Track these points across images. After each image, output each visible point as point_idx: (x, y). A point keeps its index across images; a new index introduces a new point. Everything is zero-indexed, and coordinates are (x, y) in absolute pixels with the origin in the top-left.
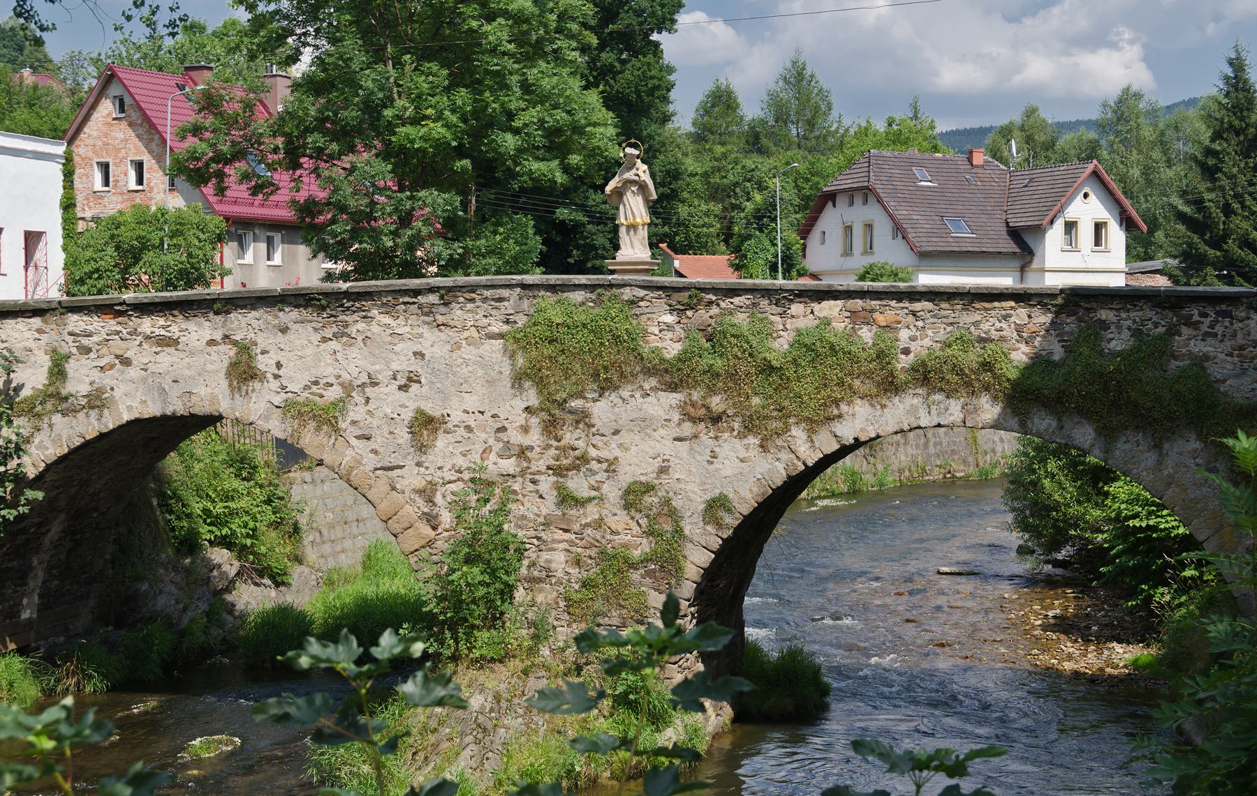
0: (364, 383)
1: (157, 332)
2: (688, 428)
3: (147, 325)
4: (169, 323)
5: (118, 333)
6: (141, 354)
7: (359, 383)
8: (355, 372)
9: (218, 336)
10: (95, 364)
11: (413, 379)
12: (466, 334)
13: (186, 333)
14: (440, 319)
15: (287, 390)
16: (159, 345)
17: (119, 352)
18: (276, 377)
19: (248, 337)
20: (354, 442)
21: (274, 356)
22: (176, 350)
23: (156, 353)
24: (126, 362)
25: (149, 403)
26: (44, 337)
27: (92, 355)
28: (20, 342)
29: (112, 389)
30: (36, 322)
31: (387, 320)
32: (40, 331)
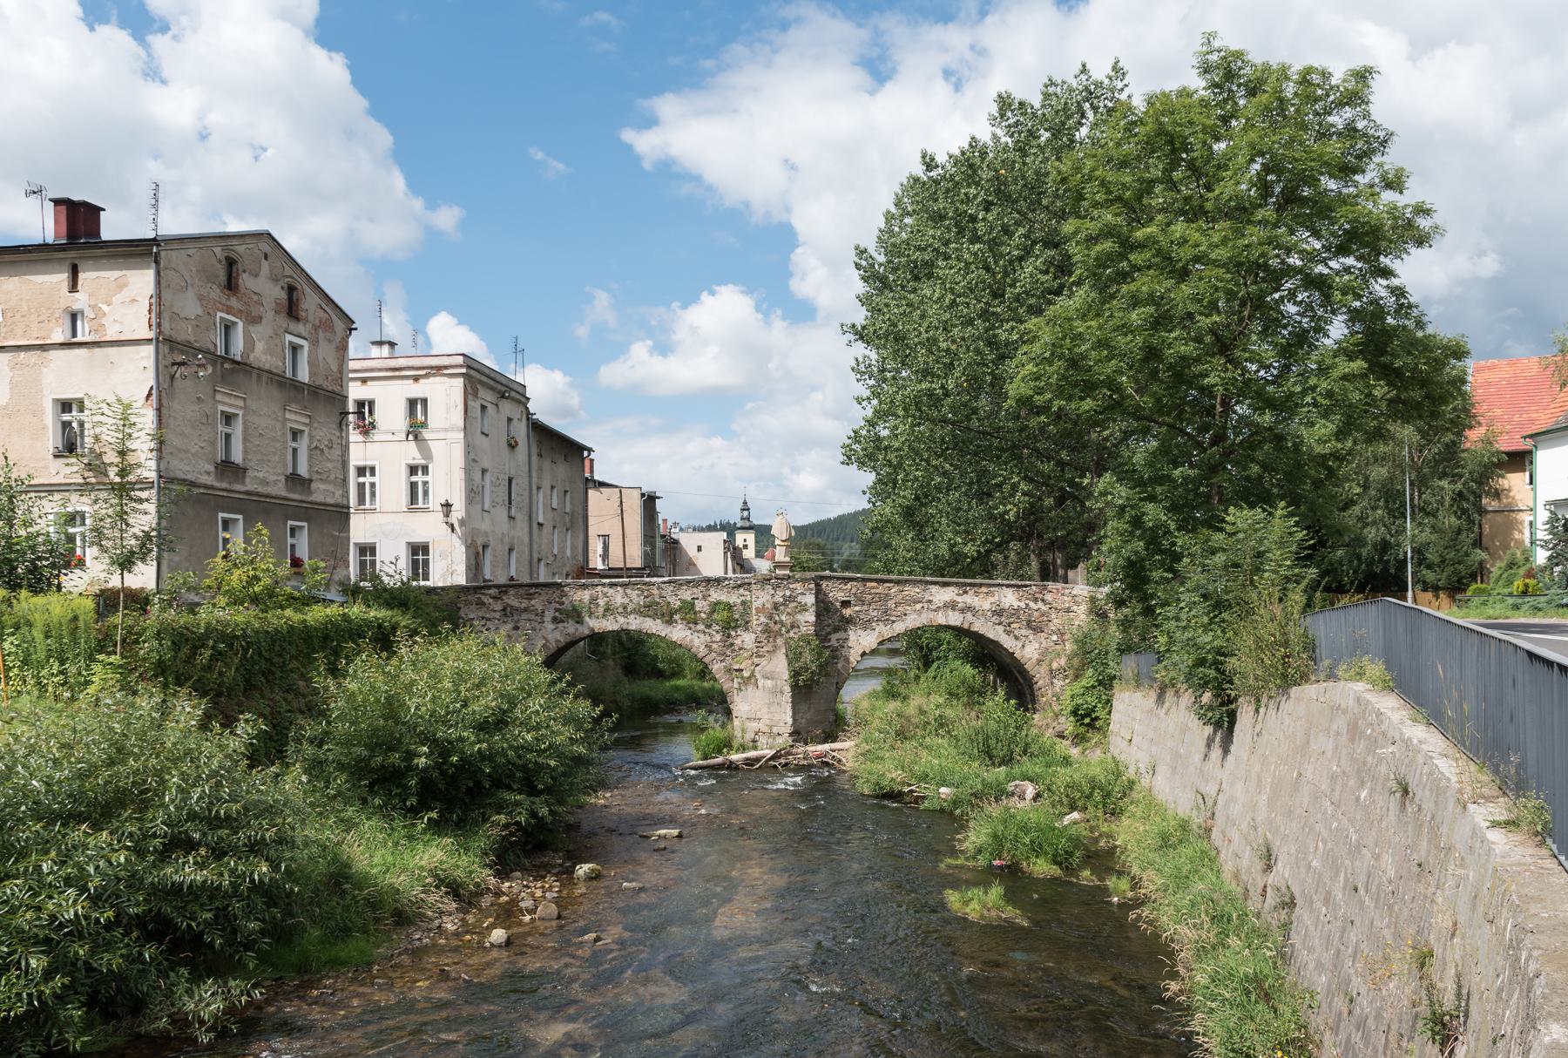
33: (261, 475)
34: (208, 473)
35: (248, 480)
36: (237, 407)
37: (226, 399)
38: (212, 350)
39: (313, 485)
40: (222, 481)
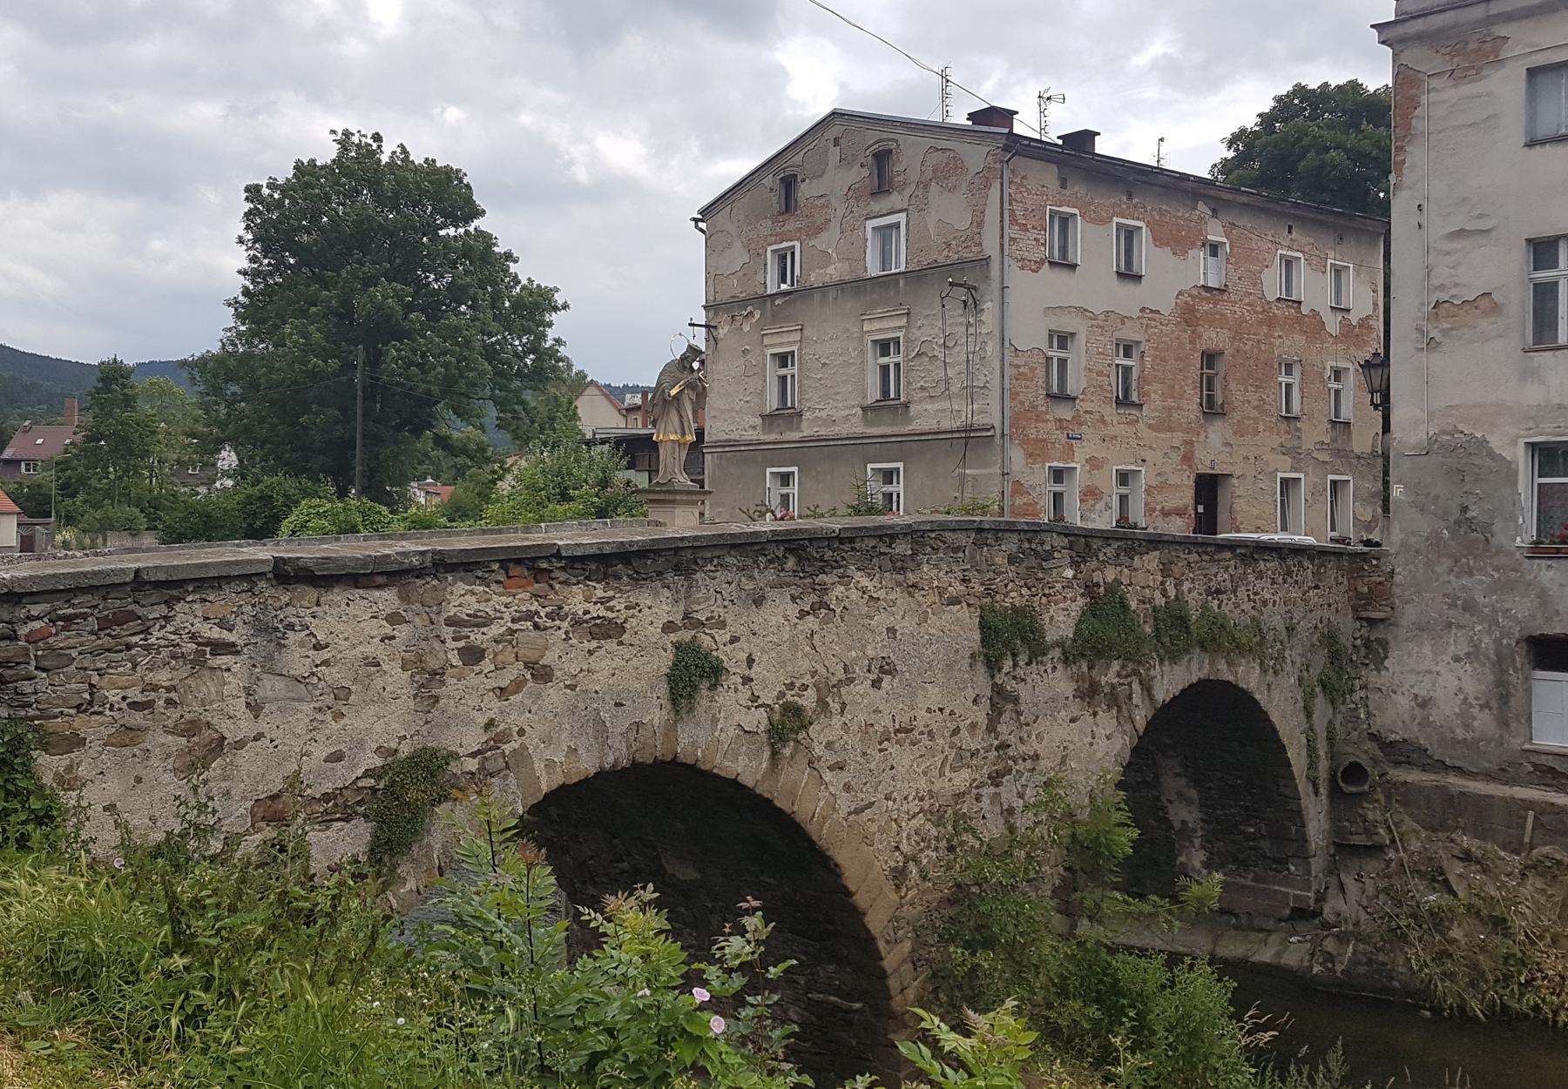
0: (840, 681)
1: (597, 611)
2: (1075, 708)
3: (578, 599)
4: (611, 593)
5: (529, 616)
6: (560, 652)
7: (834, 680)
8: (832, 662)
9: (678, 618)
10: (491, 684)
11: (887, 668)
12: (930, 599)
13: (635, 612)
14: (912, 578)
15: (760, 702)
16: (593, 636)
17: (532, 655)
18: (747, 680)
19: (715, 613)
20: (828, 776)
21: (745, 646)
22: (621, 643)
23: (590, 653)
24: (543, 674)
25: (581, 751)
26: (402, 632)
27: (487, 665)
28: (354, 646)
29: (521, 732)
30: (387, 599)
31: (865, 582)
32: (393, 619)
33: (823, 414)
34: (754, 428)
35: (804, 424)
36: (790, 343)
37: (776, 340)
38: (760, 291)
39: (913, 409)
40: (771, 432)
